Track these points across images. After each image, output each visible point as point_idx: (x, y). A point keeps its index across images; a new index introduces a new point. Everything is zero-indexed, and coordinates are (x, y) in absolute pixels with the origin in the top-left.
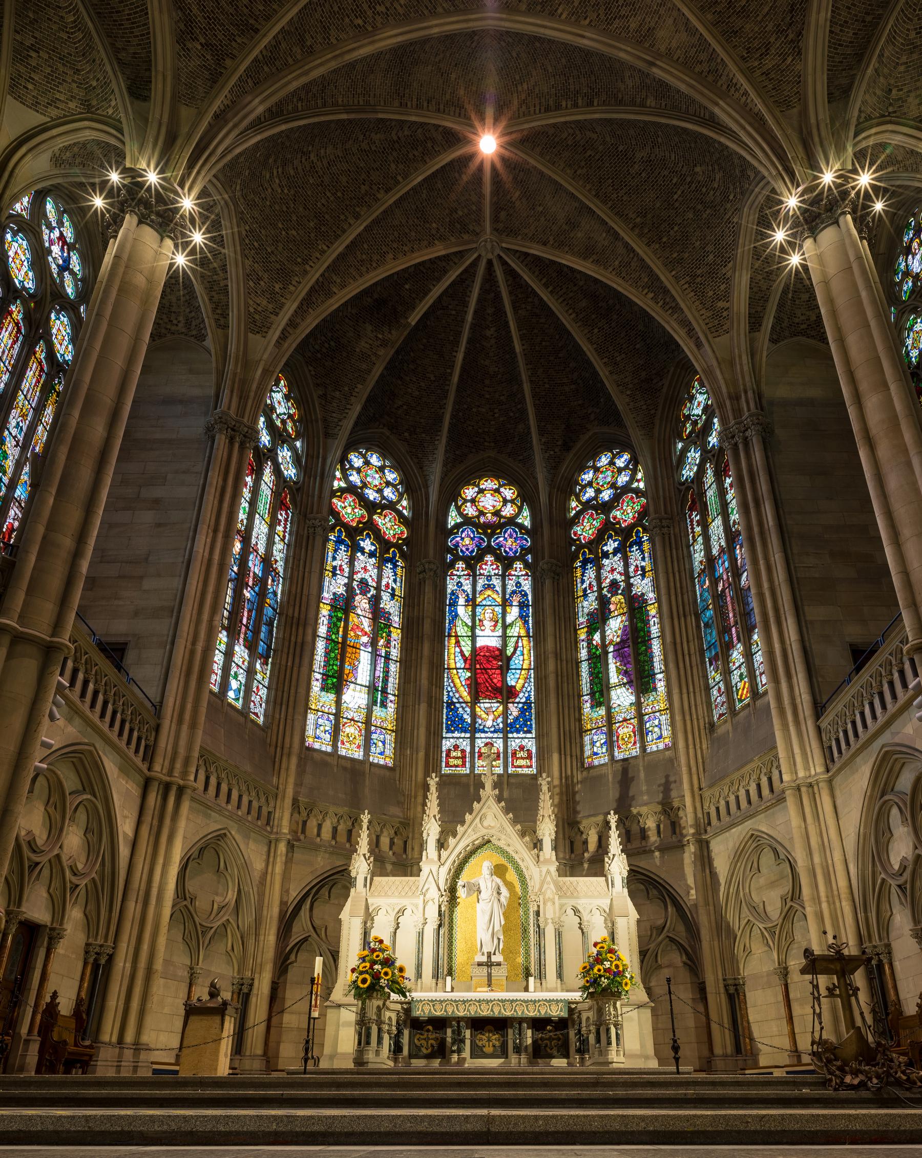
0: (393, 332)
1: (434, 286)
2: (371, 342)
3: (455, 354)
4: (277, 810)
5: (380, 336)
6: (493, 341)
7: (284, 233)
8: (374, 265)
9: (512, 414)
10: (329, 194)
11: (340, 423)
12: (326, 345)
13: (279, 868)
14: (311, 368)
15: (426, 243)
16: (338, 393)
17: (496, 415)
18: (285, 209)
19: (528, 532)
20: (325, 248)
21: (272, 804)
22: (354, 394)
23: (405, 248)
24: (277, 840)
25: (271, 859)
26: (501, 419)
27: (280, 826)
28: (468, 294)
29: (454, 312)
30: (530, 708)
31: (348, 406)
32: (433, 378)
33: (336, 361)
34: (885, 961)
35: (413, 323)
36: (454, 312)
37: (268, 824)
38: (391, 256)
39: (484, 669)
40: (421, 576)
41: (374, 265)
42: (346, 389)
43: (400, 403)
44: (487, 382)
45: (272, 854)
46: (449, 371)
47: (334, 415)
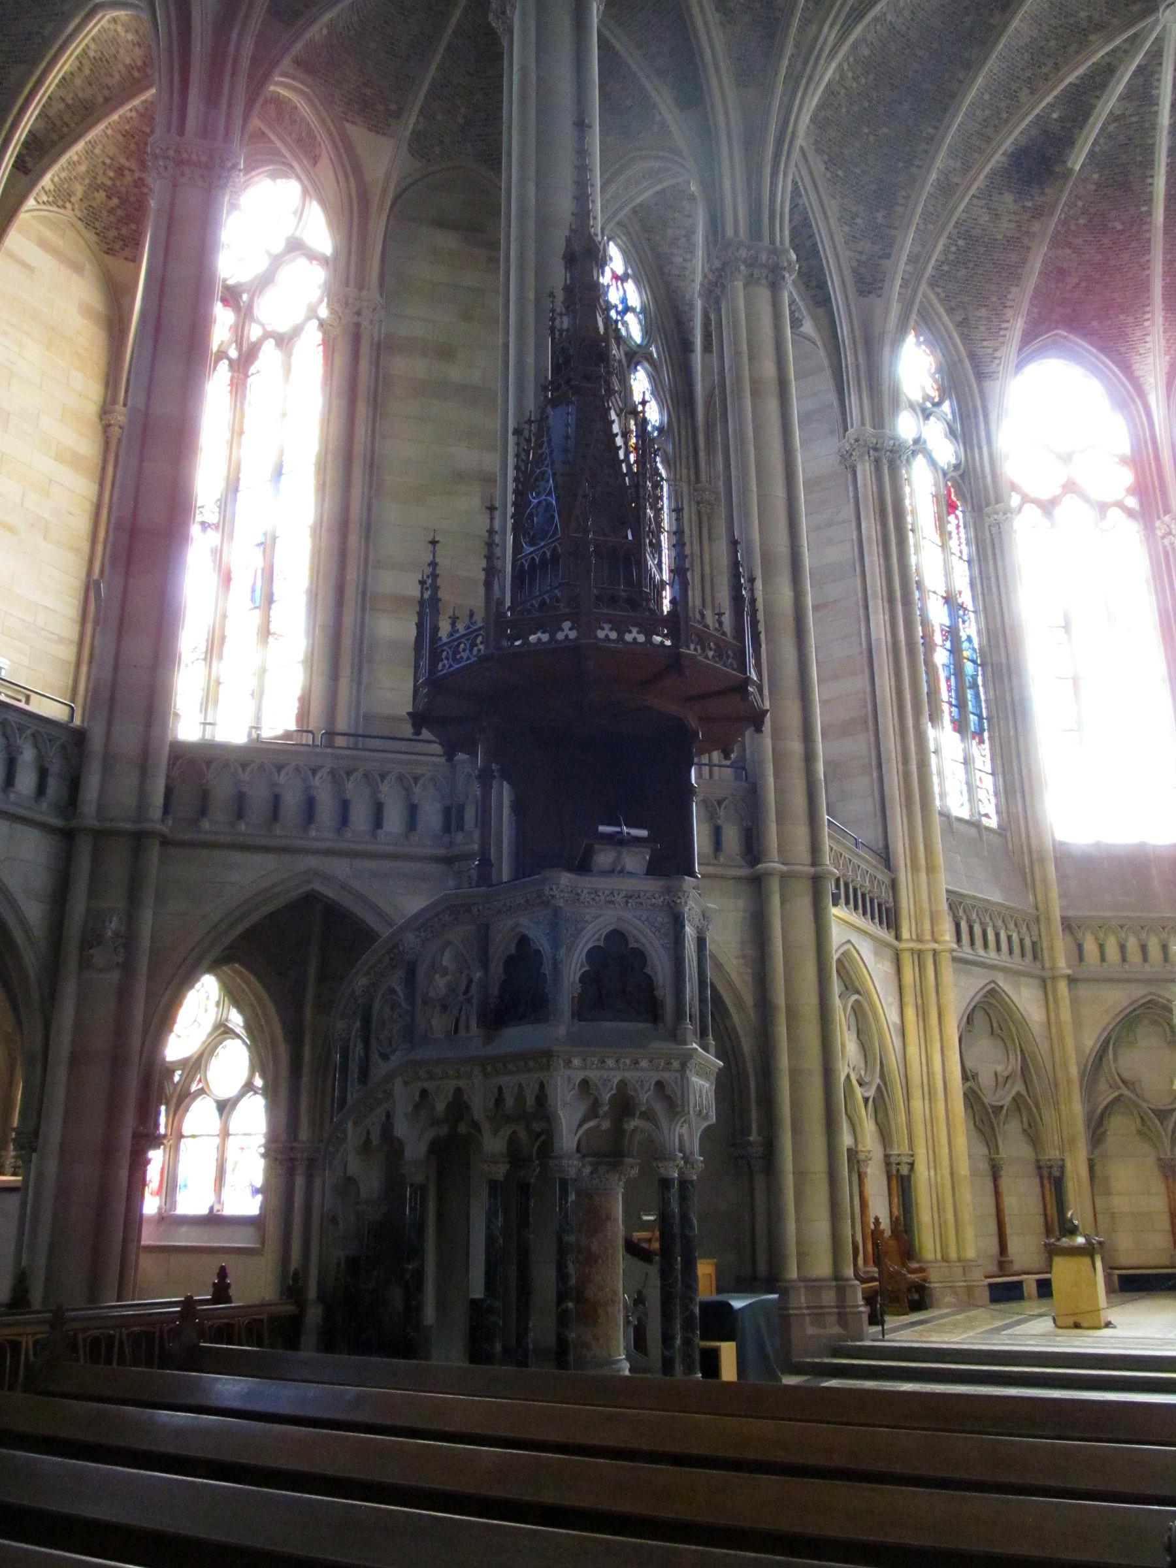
0: (1047, 191)
2: (1018, 218)
3: (1149, 180)
4: (1044, 938)
5: (1029, 204)
7: (872, 138)
8: (1004, 116)
10: (920, 53)
11: (997, 354)
12: (953, 249)
13: (1066, 1015)
14: (939, 290)
15: (1073, 48)
16: (983, 310)
18: (867, 105)
20: (931, 130)
21: (1035, 932)
22: (1009, 303)
23: (1044, 70)
24: (1054, 978)
25: (1051, 1005)
27: (1052, 958)
31: (1005, 325)
32: (1119, 227)
33: (971, 265)
35: (1077, 167)
37: (1035, 957)
38: (1026, 91)
40: (1166, 541)
41: (1004, 116)
42: (994, 299)
43: (1076, 280)
45: (1051, 998)
46: (1144, 209)
47: (985, 344)
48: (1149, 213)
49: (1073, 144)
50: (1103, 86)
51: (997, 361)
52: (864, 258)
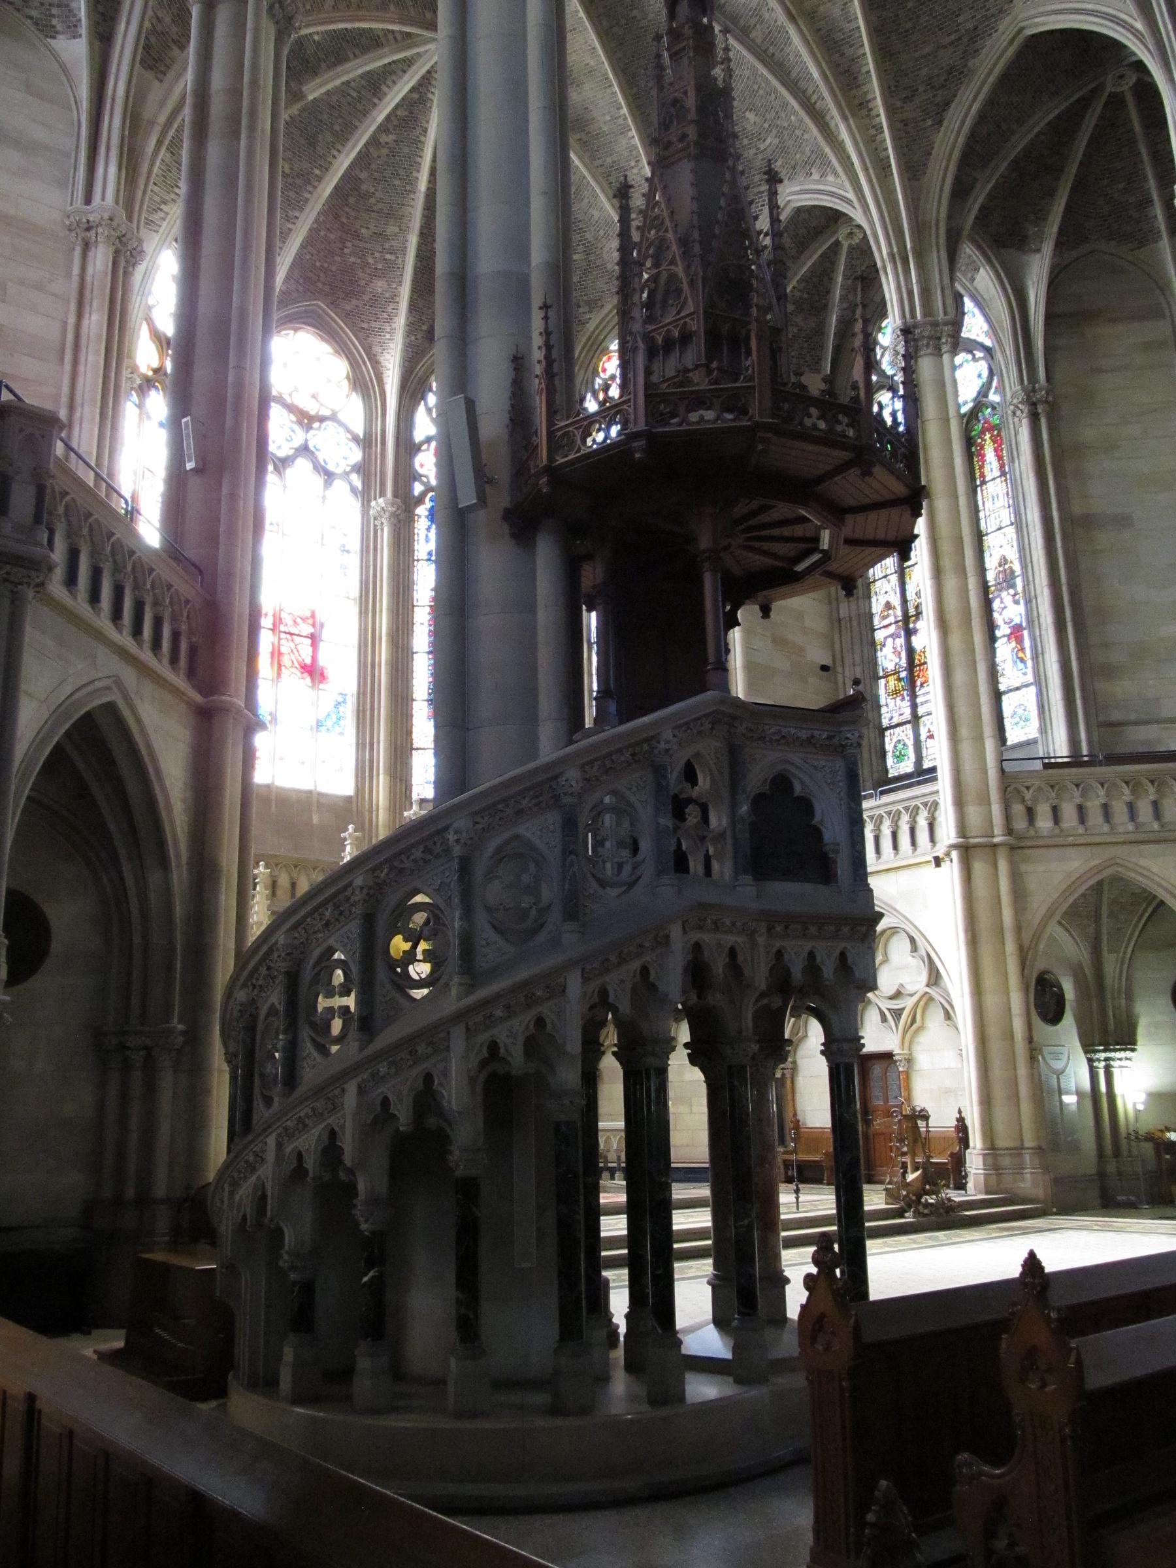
1: (356, 56)
3: (335, 153)
6: (385, 151)
9: (371, 261)
17: (346, 251)
19: (355, 439)
26: (352, 259)
28: (389, 83)
29: (354, 94)
30: (344, 702)
34: (788, 1075)
35: (310, 97)
36: (354, 94)
39: (291, 634)
44: (352, 200)
46: (317, 172)
48: (320, 179)
49: (315, 74)
50: (365, 50)
51: (161, 214)
52: (159, 28)
